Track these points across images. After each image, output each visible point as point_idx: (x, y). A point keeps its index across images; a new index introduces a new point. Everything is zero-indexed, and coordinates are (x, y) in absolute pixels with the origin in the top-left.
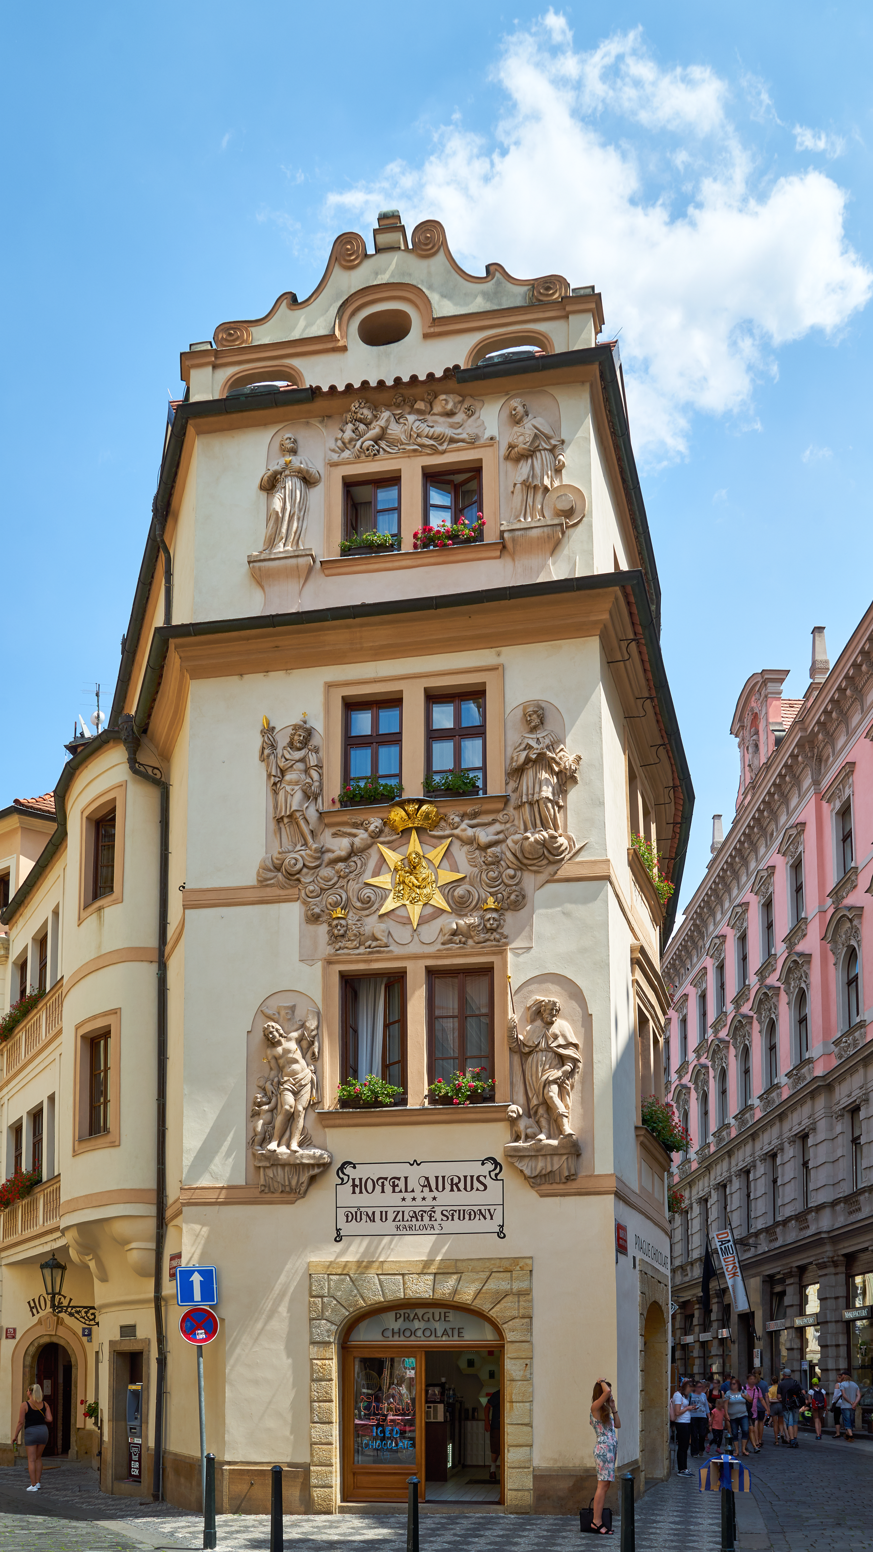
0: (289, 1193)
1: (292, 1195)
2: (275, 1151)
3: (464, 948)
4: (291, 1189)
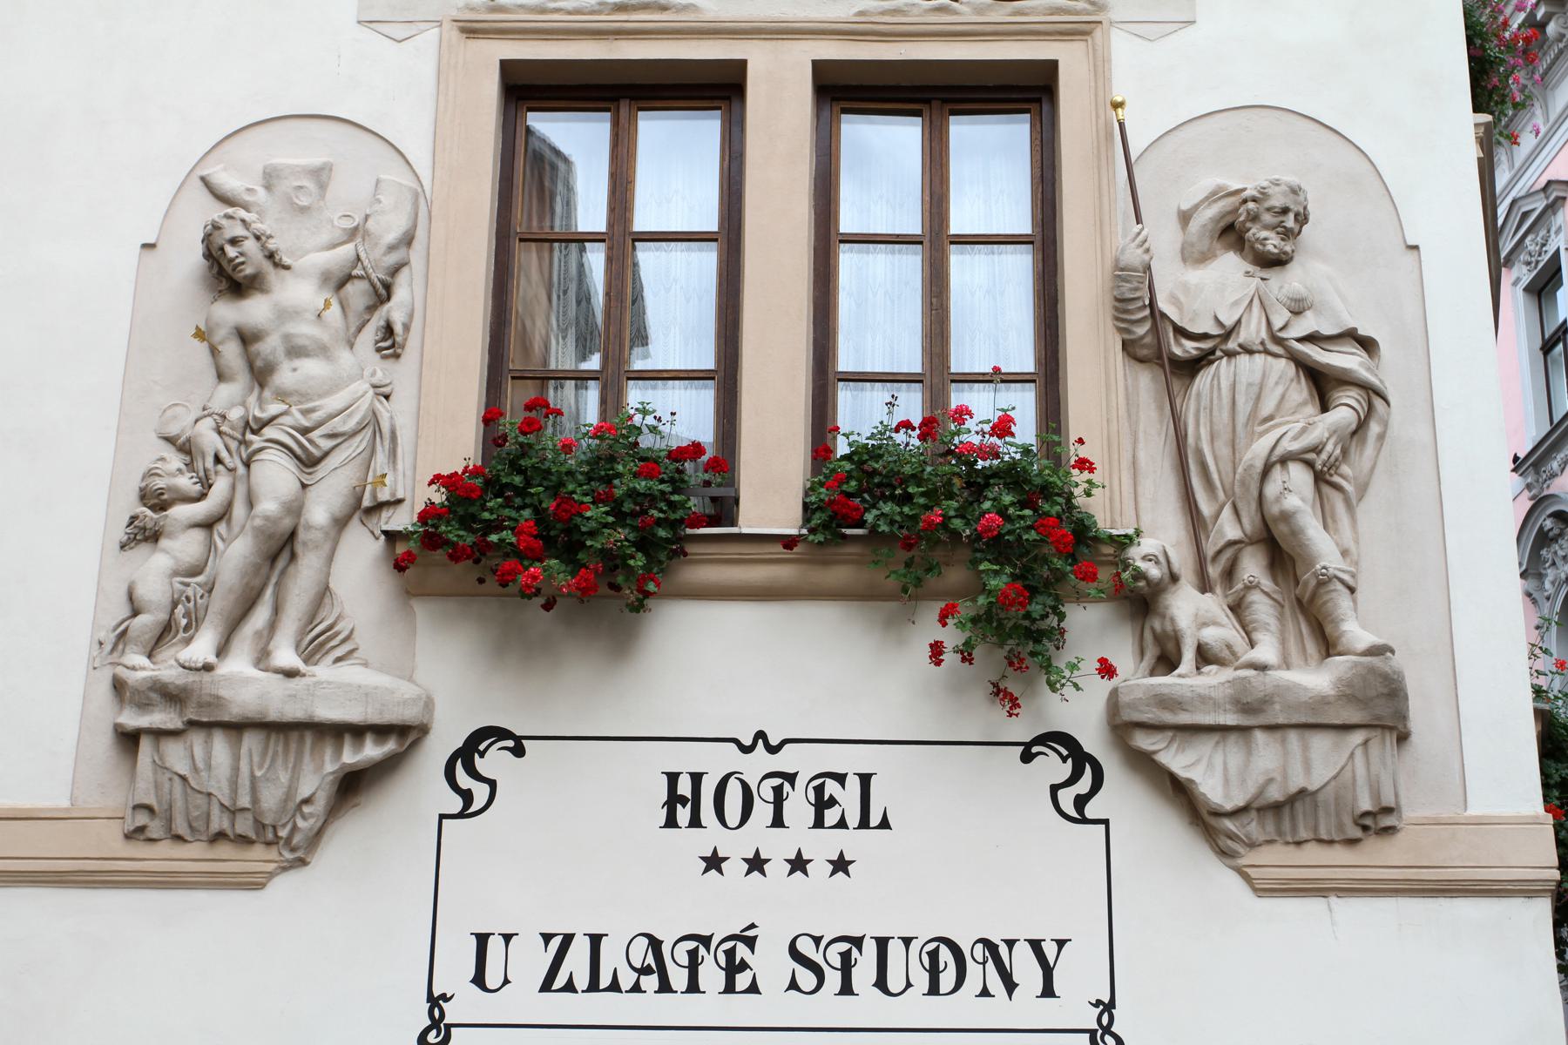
0: (244, 841)
1: (258, 851)
2: (208, 668)
3: (956, 13)
4: (260, 826)
